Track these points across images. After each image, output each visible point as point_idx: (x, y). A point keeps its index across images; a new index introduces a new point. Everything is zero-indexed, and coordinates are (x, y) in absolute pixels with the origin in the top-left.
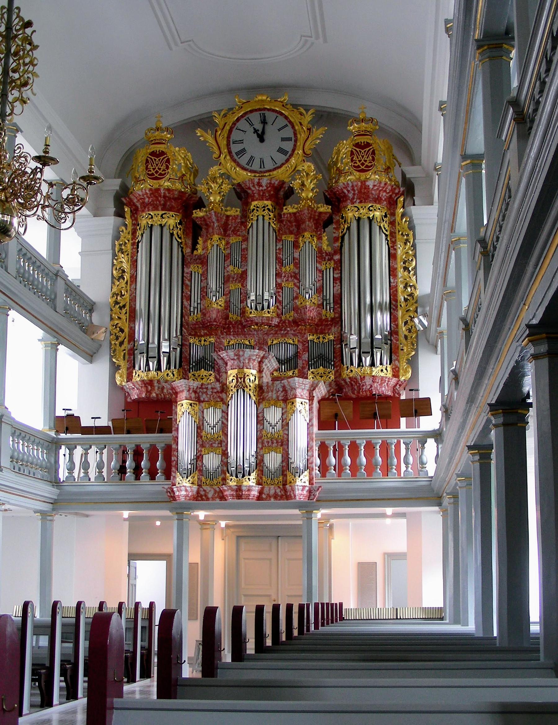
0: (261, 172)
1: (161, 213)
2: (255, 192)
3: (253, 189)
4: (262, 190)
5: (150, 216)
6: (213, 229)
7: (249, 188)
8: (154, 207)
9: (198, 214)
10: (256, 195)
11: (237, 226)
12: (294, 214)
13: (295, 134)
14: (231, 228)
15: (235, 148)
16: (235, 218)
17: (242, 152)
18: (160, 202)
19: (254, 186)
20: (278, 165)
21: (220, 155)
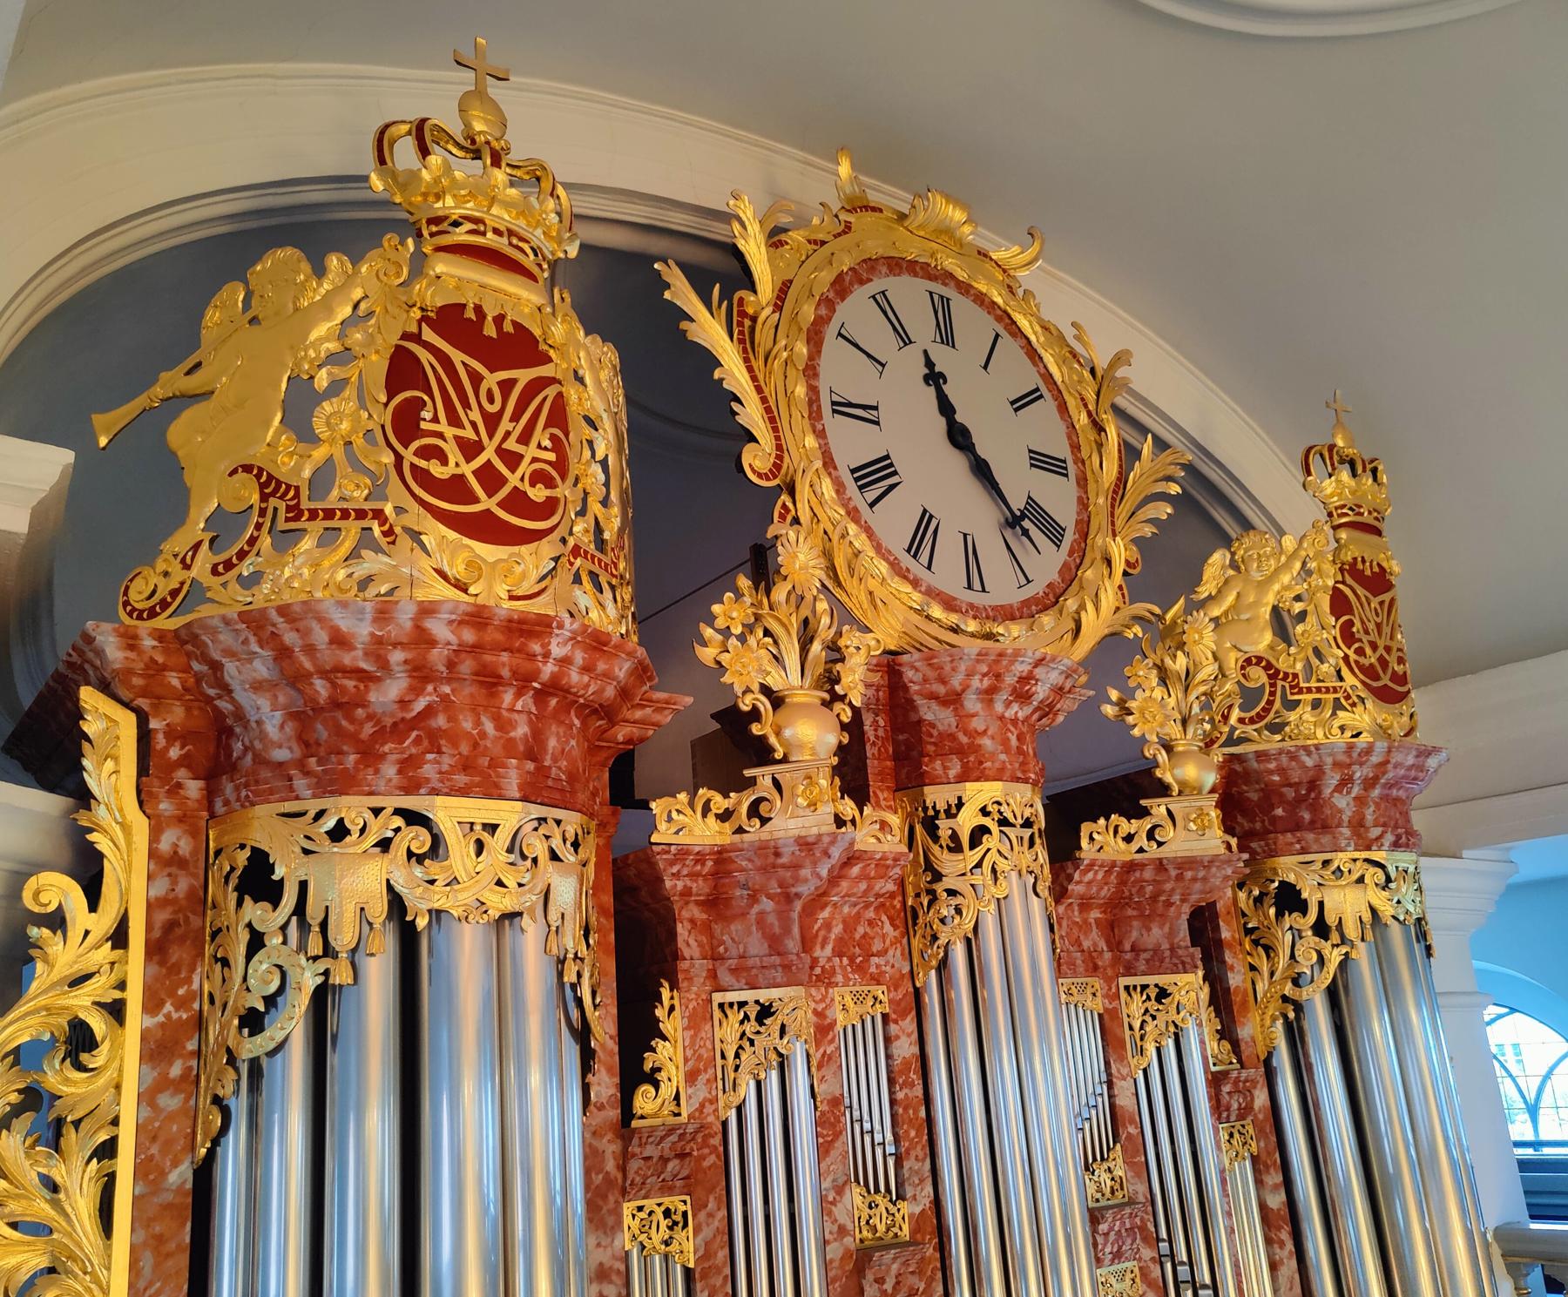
0: (975, 612)
1: (510, 814)
2: (977, 724)
3: (972, 703)
4: (1014, 721)
5: (418, 839)
6: (775, 944)
7: (953, 700)
8: (466, 766)
9: (685, 824)
10: (987, 742)
11: (858, 916)
12: (1131, 867)
13: (1076, 448)
14: (828, 926)
15: (855, 443)
16: (883, 865)
17: (877, 474)
18: (503, 725)
19: (989, 694)
20: (1037, 589)
21: (780, 457)
